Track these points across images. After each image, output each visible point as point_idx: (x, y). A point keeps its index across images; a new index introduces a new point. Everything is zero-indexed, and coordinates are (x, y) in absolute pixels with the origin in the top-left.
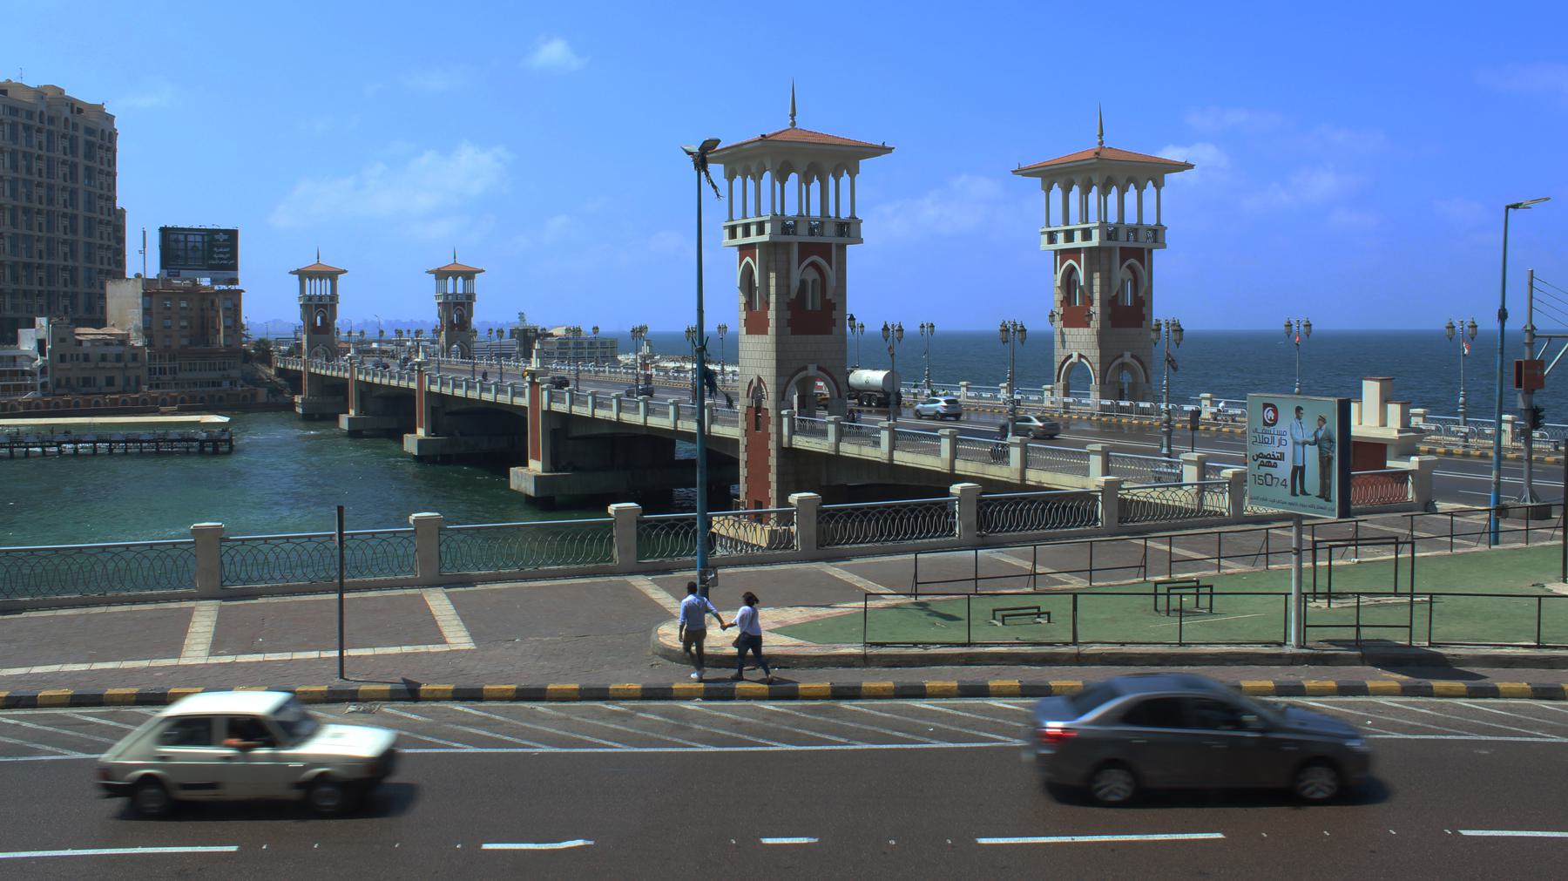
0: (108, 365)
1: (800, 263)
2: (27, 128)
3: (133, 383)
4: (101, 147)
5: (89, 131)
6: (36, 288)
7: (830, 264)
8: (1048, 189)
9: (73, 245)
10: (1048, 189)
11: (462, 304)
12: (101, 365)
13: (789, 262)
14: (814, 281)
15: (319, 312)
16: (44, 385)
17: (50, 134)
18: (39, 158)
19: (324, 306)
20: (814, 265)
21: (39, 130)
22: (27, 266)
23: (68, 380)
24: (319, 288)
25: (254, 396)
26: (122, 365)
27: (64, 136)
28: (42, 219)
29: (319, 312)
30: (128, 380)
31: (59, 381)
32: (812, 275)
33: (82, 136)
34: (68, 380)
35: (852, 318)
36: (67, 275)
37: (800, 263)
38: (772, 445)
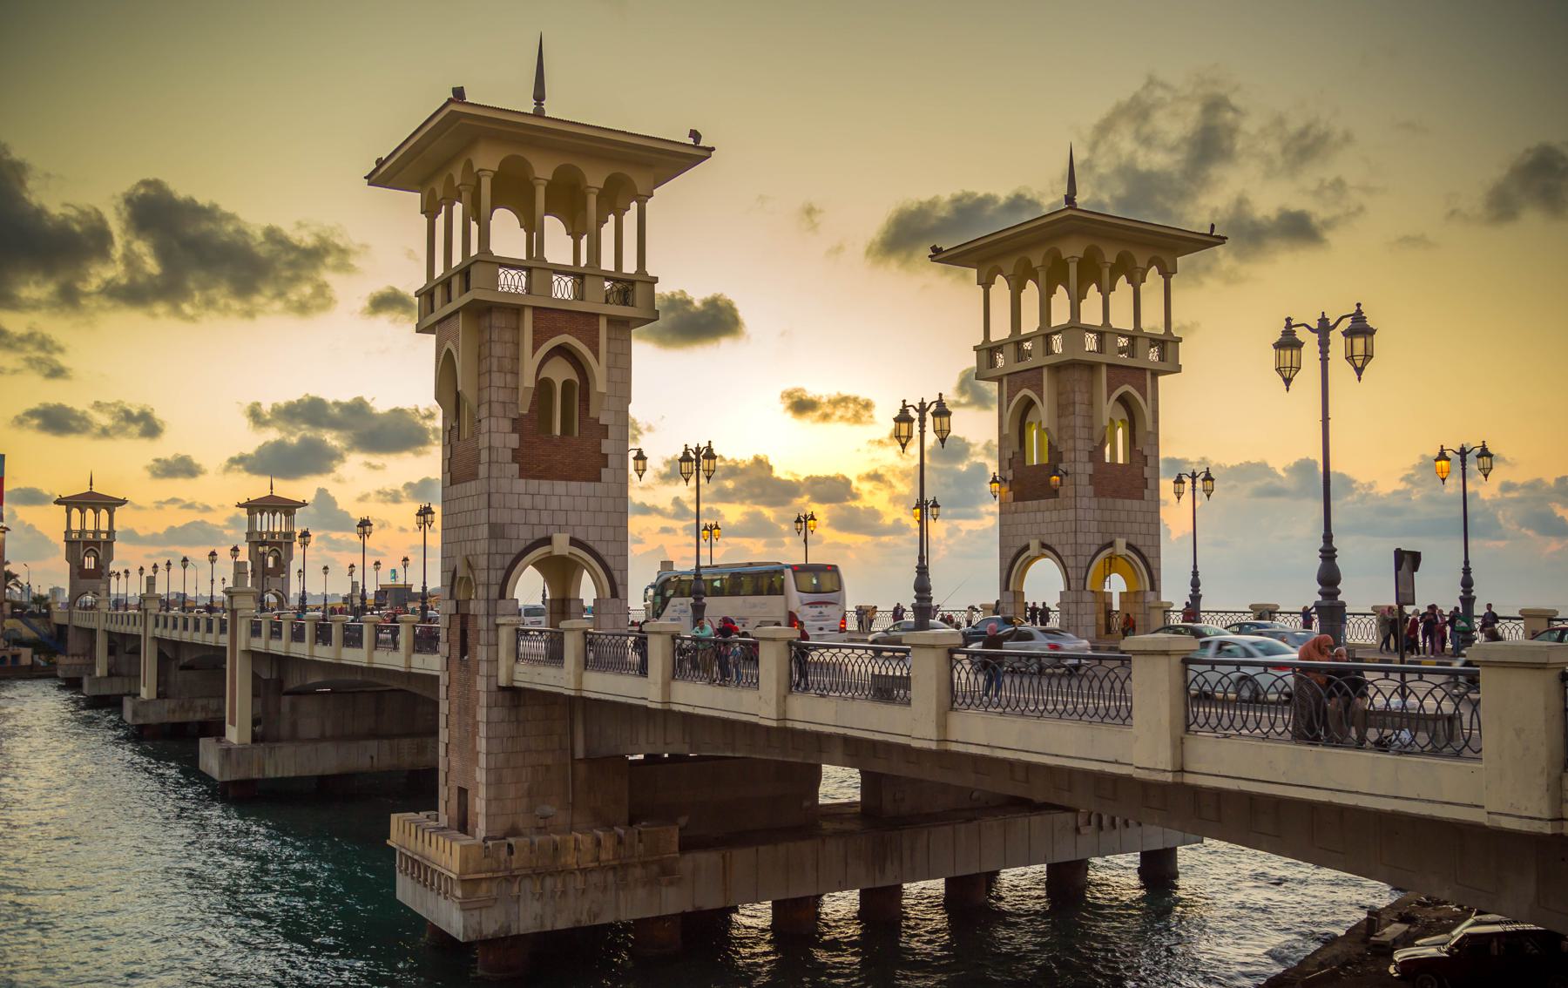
1: (535, 348)
7: (596, 354)
8: (986, 283)
10: (986, 283)
11: (279, 544)
13: (517, 344)
14: (567, 384)
15: (90, 555)
19: (97, 544)
20: (563, 351)
24: (91, 521)
25: (16, 657)
29: (90, 555)
32: (560, 373)
35: (640, 456)
37: (535, 348)
38: (481, 684)
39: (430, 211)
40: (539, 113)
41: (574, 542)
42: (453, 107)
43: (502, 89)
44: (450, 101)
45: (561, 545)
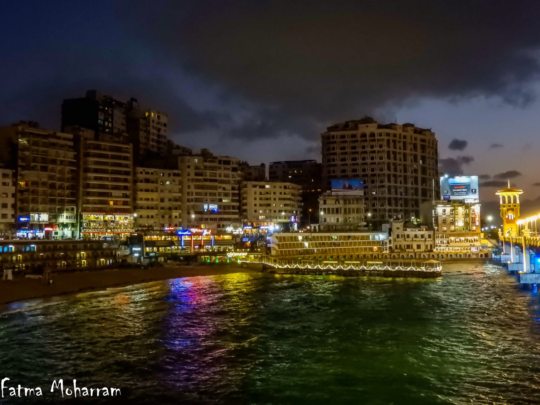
0: (417, 239)
2: (394, 141)
3: (429, 248)
4: (429, 147)
5: (423, 141)
6: (399, 208)
9: (416, 190)
12: (414, 239)
16: (390, 248)
17: (405, 143)
18: (400, 153)
21: (399, 142)
22: (396, 199)
23: (400, 246)
26: (424, 239)
27: (411, 143)
28: (402, 179)
30: (427, 246)
31: (396, 246)
33: (419, 143)
34: (400, 246)
36: (413, 202)
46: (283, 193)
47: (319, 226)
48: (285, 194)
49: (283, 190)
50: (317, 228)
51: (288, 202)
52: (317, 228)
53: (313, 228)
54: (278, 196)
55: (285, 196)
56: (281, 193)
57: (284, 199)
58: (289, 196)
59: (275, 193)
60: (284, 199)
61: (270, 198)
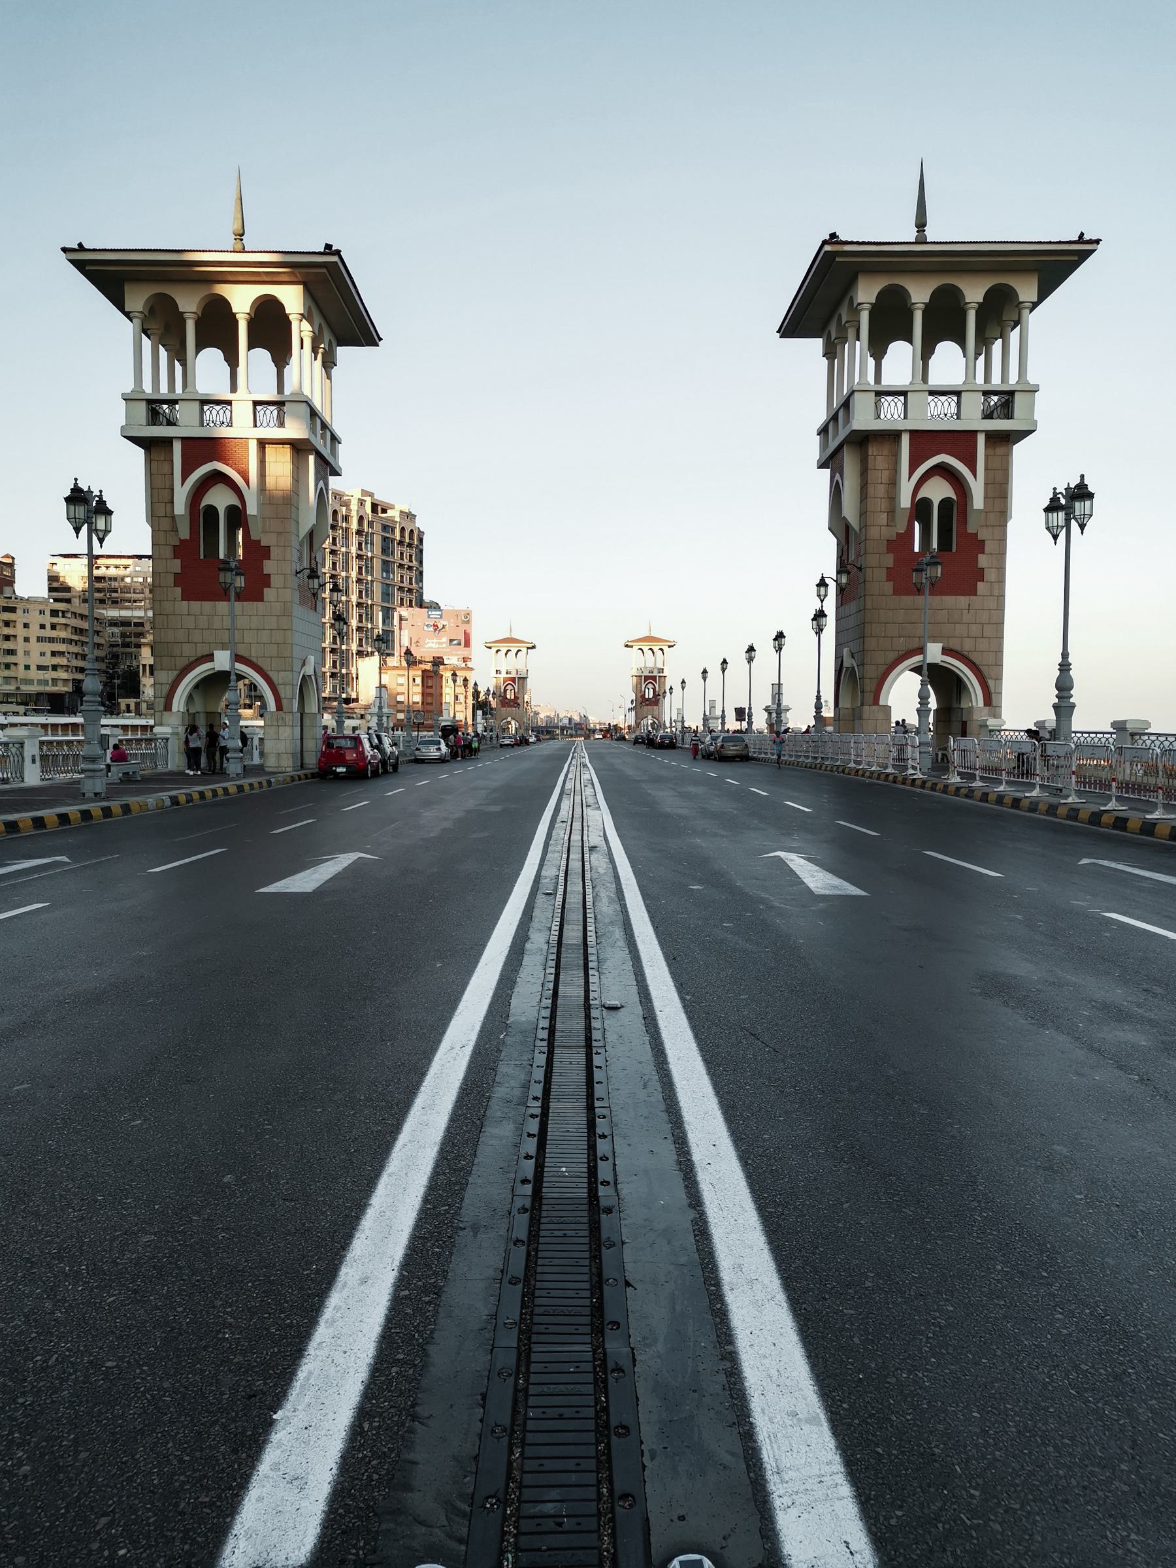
39: (830, 353)
40: (921, 240)
41: (238, 658)
42: (827, 248)
43: (885, 224)
44: (824, 243)
45: (222, 660)
46: (48, 626)
47: (137, 705)
48: (53, 627)
49: (48, 620)
50: (132, 707)
51: (62, 647)
52: (132, 707)
53: (123, 707)
54: (35, 631)
55: (54, 634)
56: (42, 627)
57: (51, 640)
58: (63, 634)
59: (26, 626)
60: (51, 640)
61: (15, 636)
